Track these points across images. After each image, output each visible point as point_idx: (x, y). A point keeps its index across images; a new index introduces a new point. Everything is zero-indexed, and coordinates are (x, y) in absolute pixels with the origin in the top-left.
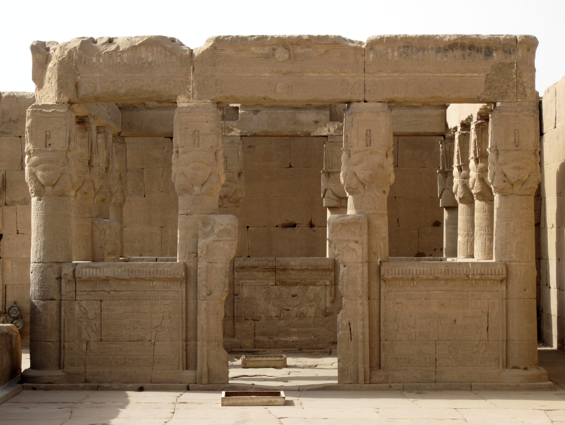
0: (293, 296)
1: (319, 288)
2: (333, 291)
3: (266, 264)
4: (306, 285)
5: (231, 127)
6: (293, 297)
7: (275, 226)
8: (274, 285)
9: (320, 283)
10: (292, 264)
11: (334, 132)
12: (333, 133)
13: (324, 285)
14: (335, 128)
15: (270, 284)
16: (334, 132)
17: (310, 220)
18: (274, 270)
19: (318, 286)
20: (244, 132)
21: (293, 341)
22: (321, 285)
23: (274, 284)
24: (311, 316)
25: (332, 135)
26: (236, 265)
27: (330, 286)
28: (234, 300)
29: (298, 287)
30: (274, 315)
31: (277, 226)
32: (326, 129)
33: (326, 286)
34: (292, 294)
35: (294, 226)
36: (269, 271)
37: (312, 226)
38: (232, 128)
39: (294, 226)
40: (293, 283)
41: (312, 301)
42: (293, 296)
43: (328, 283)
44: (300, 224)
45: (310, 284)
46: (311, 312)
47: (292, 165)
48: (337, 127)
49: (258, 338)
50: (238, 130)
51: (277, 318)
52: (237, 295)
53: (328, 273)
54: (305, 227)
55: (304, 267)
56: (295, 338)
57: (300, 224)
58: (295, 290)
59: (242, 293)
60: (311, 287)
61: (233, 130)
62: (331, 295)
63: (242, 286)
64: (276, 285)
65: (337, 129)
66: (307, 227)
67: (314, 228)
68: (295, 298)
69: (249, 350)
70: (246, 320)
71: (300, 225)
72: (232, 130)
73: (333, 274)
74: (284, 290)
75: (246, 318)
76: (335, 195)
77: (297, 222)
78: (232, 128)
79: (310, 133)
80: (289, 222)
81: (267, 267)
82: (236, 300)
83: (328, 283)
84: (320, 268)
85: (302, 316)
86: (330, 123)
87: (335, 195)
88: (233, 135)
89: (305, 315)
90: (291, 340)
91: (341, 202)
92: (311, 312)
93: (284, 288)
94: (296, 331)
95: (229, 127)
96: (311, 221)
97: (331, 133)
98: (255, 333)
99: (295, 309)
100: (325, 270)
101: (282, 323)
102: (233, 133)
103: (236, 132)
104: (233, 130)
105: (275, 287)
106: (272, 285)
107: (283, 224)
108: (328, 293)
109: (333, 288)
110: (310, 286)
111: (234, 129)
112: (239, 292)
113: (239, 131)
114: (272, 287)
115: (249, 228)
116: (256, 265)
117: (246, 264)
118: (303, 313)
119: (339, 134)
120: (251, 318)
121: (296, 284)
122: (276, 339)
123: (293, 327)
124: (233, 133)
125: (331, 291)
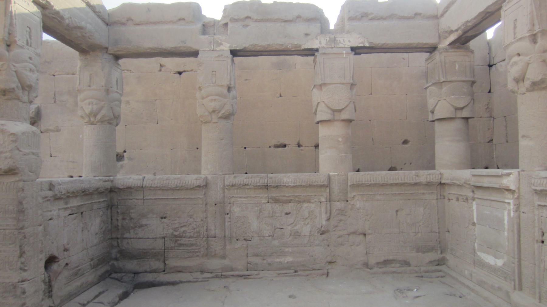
0: (287, 214)
1: (313, 205)
2: (329, 208)
3: (258, 181)
4: (300, 202)
5: (220, 42)
6: (287, 216)
7: (269, 146)
8: (266, 203)
9: (315, 200)
10: (285, 180)
11: (325, 44)
12: (325, 46)
13: (319, 202)
14: (326, 40)
15: (263, 202)
16: (325, 44)
17: (298, 141)
18: (266, 187)
19: (313, 203)
20: (233, 46)
21: (288, 262)
22: (316, 202)
23: (267, 201)
24: (306, 235)
25: (324, 48)
26: (227, 183)
27: (326, 203)
28: (225, 218)
29: (291, 204)
30: (267, 235)
31: (270, 147)
32: (317, 42)
33: (321, 202)
34: (286, 212)
35: (285, 146)
36: (261, 188)
37: (299, 146)
38: (221, 42)
39: (285, 146)
40: (286, 200)
41: (306, 218)
42: (287, 214)
43: (323, 200)
44: (290, 144)
45: (304, 201)
46: (306, 230)
47: (282, 95)
48: (328, 39)
49: (251, 259)
50: (227, 44)
51: (271, 237)
52: (228, 214)
53: (323, 189)
54: (294, 147)
55: (298, 184)
56: (289, 259)
57: (290, 144)
58: (289, 207)
59: (233, 211)
60: (305, 205)
61: (222, 44)
62: (326, 213)
63: (233, 204)
64: (268, 202)
65: (329, 41)
66: (296, 147)
67: (301, 148)
68: (289, 215)
69: (241, 273)
70: (237, 240)
71: (289, 146)
72: (221, 44)
73: (328, 190)
74: (278, 207)
75: (237, 239)
76: (329, 107)
77: (286, 143)
78: (221, 42)
79: (300, 46)
80: (280, 143)
81: (258, 184)
82: (227, 220)
83: (323, 200)
84: (315, 184)
85: (297, 235)
86: (321, 36)
87: (329, 107)
88: (222, 49)
89: (300, 233)
90: (286, 261)
91: (334, 115)
92: (306, 230)
93: (277, 205)
94: (291, 251)
95: (218, 41)
96: (299, 142)
97: (322, 45)
98: (247, 254)
99: (289, 228)
100: (321, 186)
101: (276, 242)
102: (222, 47)
103: (226, 47)
104: (222, 44)
105: (268, 205)
106: (264, 203)
107: (275, 145)
108: (323, 209)
109: (329, 205)
110: (304, 203)
111: (223, 43)
112: (230, 211)
113: (228, 45)
114: (264, 205)
115: (246, 149)
116: (247, 183)
117: (237, 182)
118: (298, 232)
119: (330, 47)
120: (243, 239)
121: (290, 201)
122: (270, 260)
123: (287, 247)
124: (222, 47)
125: (326, 208)
